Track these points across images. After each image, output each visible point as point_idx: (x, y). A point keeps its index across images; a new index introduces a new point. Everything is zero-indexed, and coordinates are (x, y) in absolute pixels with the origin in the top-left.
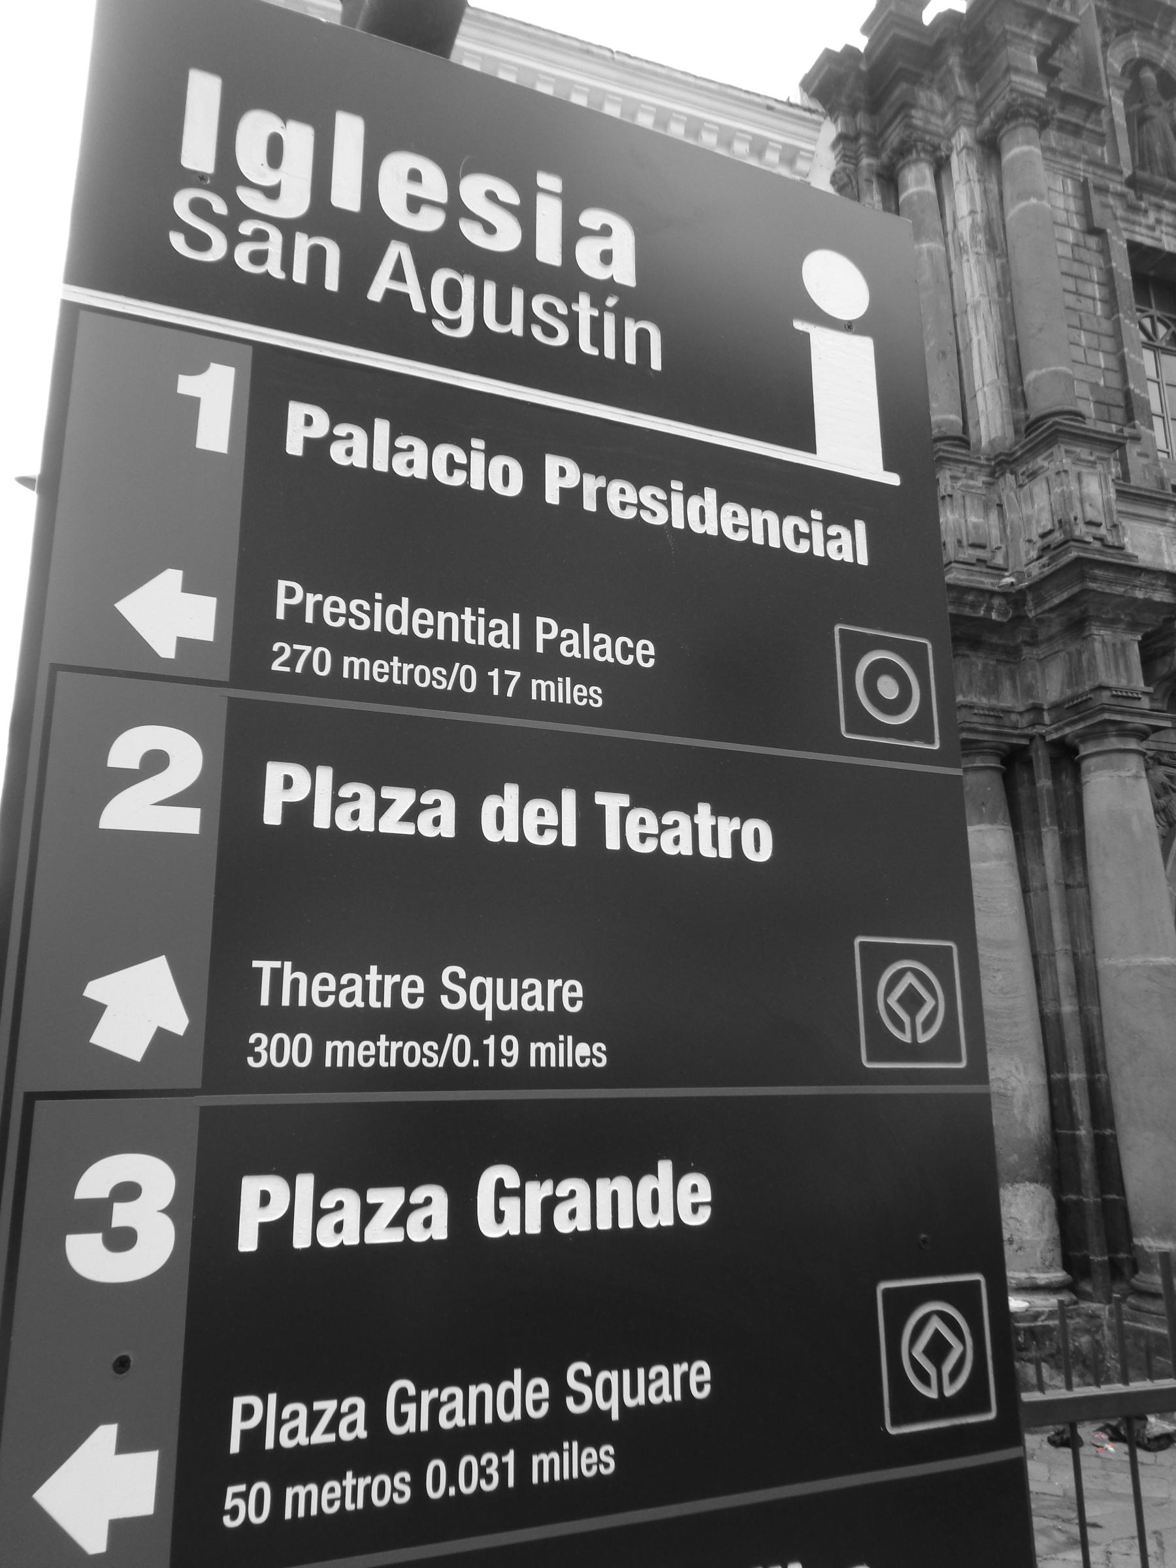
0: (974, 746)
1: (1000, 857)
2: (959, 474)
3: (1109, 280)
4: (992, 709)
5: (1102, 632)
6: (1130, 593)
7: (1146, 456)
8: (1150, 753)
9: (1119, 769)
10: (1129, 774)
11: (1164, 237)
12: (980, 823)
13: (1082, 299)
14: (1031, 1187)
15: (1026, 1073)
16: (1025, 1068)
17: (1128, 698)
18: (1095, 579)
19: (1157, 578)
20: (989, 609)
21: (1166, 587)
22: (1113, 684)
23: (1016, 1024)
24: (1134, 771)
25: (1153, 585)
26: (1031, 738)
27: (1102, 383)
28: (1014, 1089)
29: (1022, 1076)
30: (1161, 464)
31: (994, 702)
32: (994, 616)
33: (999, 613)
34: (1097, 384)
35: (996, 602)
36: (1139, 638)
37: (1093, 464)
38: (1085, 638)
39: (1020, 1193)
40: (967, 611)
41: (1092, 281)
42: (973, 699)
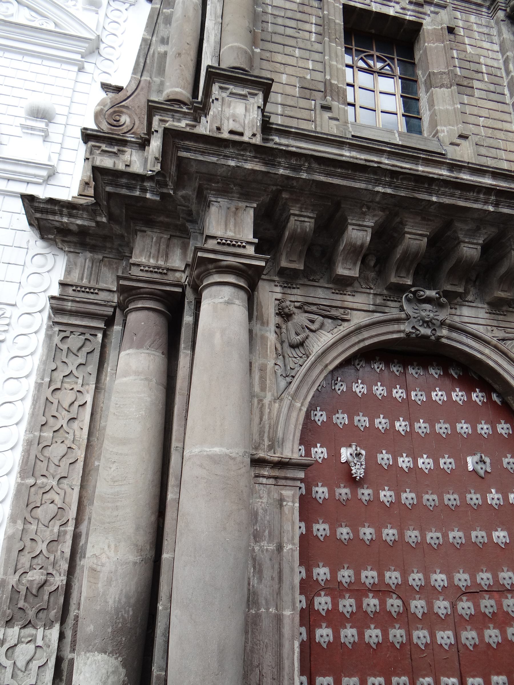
0: (134, 292)
1: (137, 373)
2: (167, 119)
3: (323, 24)
4: (158, 268)
5: (219, 200)
6: (223, 161)
7: (337, 119)
8: (297, 304)
9: (215, 297)
10: (221, 300)
11: (373, 4)
12: (129, 348)
13: (300, 31)
14: (100, 657)
15: (116, 551)
16: (116, 546)
17: (234, 245)
18: (188, 150)
19: (245, 150)
20: (144, 190)
21: (255, 157)
22: (219, 233)
23: (117, 508)
24: (226, 299)
25: (243, 155)
26: (183, 287)
27: (308, 77)
28: (103, 565)
29: (112, 554)
30: (350, 125)
31: (161, 263)
32: (148, 196)
33: (152, 192)
34: (305, 78)
35: (147, 184)
36: (255, 205)
37: (244, 97)
38: (209, 207)
39: (89, 662)
40: (124, 191)
41: (312, 23)
42: (143, 260)
